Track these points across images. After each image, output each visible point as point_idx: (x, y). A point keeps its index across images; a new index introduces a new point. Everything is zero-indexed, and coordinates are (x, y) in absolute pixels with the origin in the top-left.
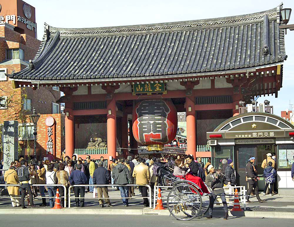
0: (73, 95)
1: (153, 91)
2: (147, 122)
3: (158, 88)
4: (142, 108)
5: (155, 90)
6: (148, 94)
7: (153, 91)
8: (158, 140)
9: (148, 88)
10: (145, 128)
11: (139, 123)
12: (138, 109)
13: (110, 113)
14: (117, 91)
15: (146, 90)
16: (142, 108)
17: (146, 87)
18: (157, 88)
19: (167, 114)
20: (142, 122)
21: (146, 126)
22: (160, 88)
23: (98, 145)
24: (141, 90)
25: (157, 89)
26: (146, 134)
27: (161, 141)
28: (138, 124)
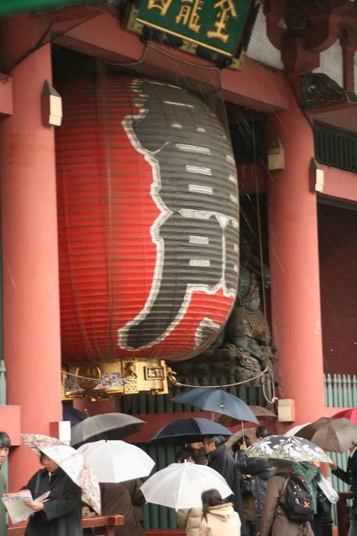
1: (203, 31)
3: (221, 25)
4: (177, 126)
5: (211, 34)
7: (203, 31)
11: (165, 213)
16: (177, 126)
20: (187, 213)
25: (215, 29)
26: (204, 289)
28: (160, 220)
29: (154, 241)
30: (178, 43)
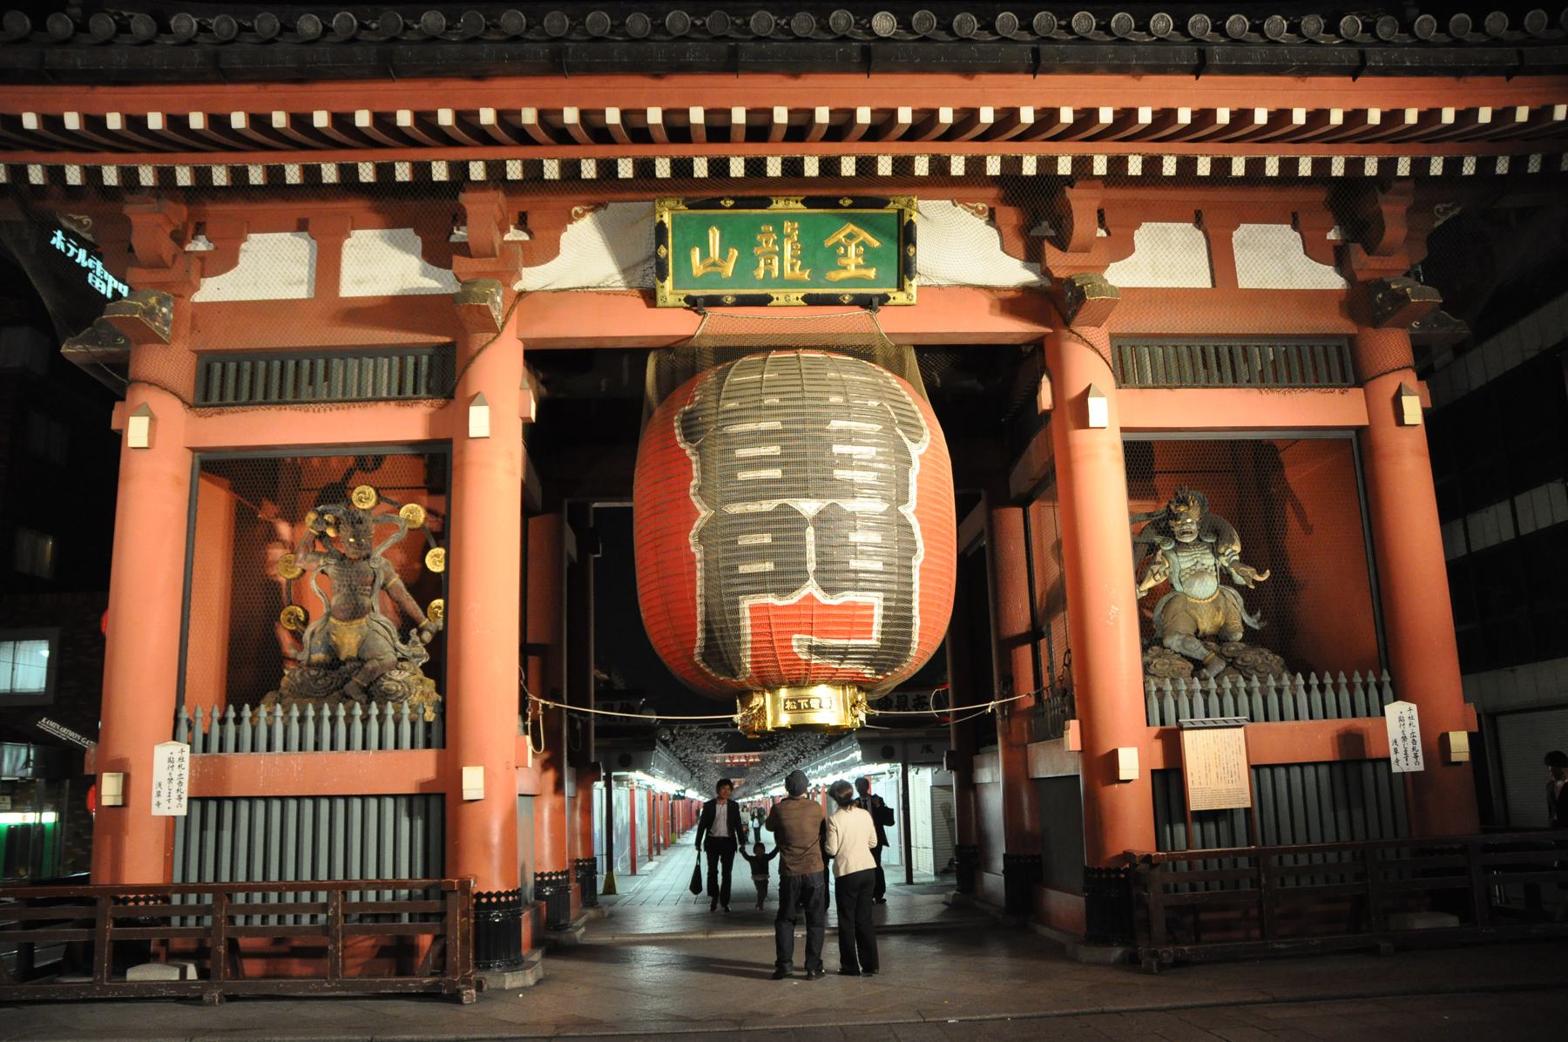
0: (198, 298)
2: (768, 506)
4: (732, 405)
6: (779, 295)
8: (843, 654)
9: (781, 254)
10: (758, 553)
12: (692, 411)
13: (479, 420)
14: (532, 278)
15: (761, 273)
16: (732, 405)
17: (767, 241)
18: (844, 261)
19: (916, 451)
21: (767, 539)
22: (870, 257)
23: (366, 691)
24: (729, 269)
26: (771, 599)
27: (869, 663)
29: (693, 549)
30: (764, 301)
